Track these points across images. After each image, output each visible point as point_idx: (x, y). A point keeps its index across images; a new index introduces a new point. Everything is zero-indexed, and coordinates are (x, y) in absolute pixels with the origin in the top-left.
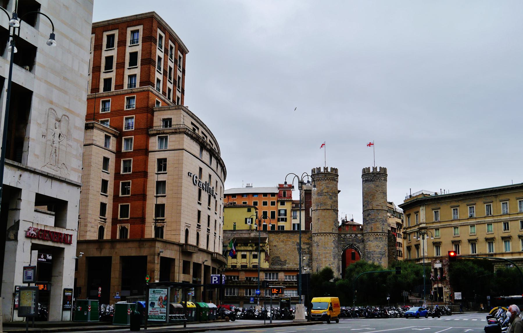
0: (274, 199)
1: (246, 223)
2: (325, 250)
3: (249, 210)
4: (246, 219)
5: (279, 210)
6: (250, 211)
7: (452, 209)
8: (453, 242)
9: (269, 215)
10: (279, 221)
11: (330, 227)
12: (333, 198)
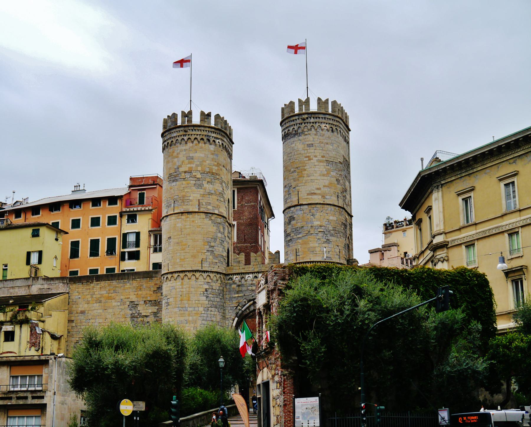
0: (115, 210)
1: (28, 262)
2: (182, 315)
3: (36, 234)
4: (29, 254)
5: (125, 236)
6: (38, 235)
7: (502, 184)
8: (507, 273)
9: (103, 247)
10: (123, 258)
11: (194, 256)
12: (206, 185)
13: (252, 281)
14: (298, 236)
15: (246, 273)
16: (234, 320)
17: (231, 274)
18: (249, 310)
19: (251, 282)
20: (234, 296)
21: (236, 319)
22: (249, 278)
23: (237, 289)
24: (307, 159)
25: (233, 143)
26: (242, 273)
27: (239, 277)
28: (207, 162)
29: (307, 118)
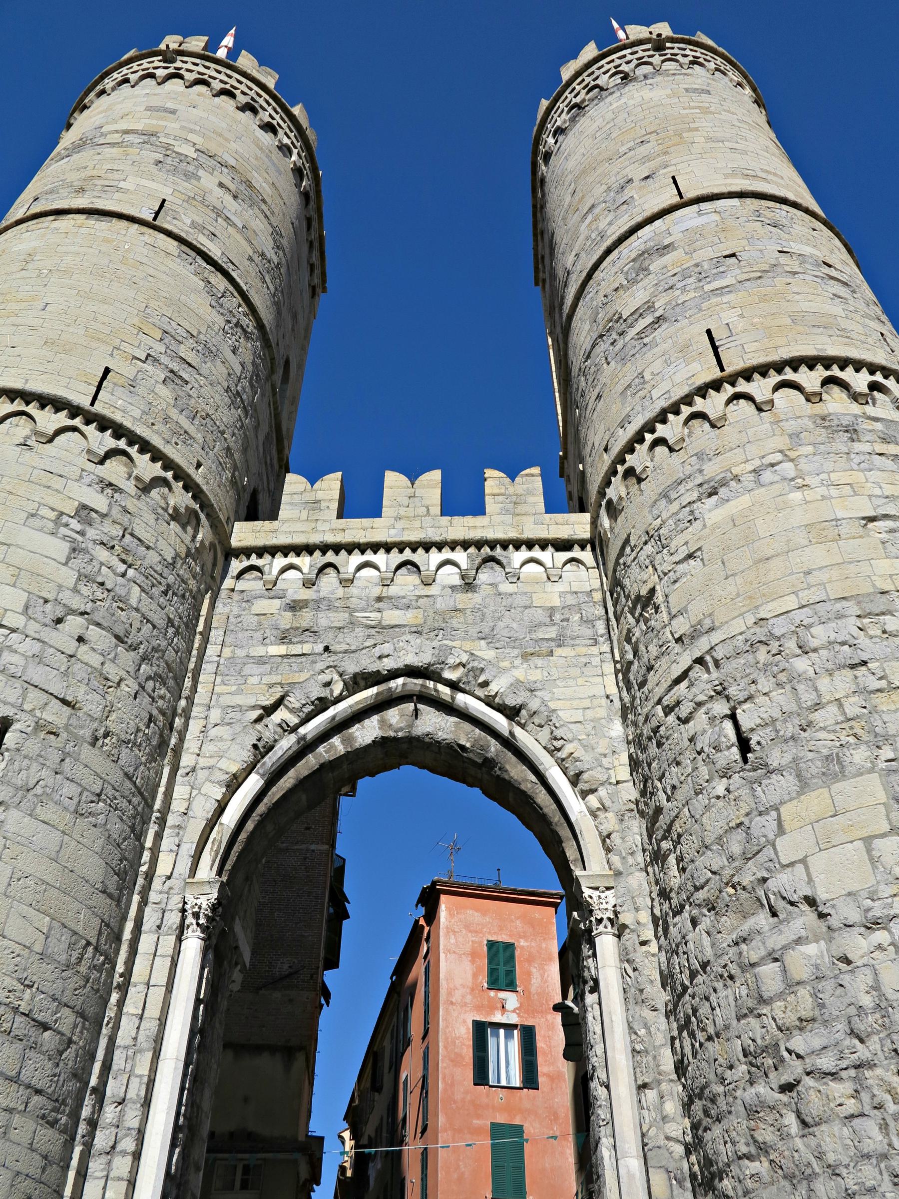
13: (386, 583)
14: (708, 288)
15: (350, 548)
16: (234, 784)
17: (260, 552)
18: (347, 741)
19: (377, 591)
20: (260, 651)
21: (254, 783)
22: (367, 572)
23: (286, 620)
24: (698, 111)
25: (324, 290)
26: (324, 548)
27: (305, 562)
28: (234, 146)
29: (673, 48)
